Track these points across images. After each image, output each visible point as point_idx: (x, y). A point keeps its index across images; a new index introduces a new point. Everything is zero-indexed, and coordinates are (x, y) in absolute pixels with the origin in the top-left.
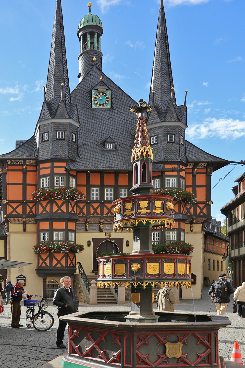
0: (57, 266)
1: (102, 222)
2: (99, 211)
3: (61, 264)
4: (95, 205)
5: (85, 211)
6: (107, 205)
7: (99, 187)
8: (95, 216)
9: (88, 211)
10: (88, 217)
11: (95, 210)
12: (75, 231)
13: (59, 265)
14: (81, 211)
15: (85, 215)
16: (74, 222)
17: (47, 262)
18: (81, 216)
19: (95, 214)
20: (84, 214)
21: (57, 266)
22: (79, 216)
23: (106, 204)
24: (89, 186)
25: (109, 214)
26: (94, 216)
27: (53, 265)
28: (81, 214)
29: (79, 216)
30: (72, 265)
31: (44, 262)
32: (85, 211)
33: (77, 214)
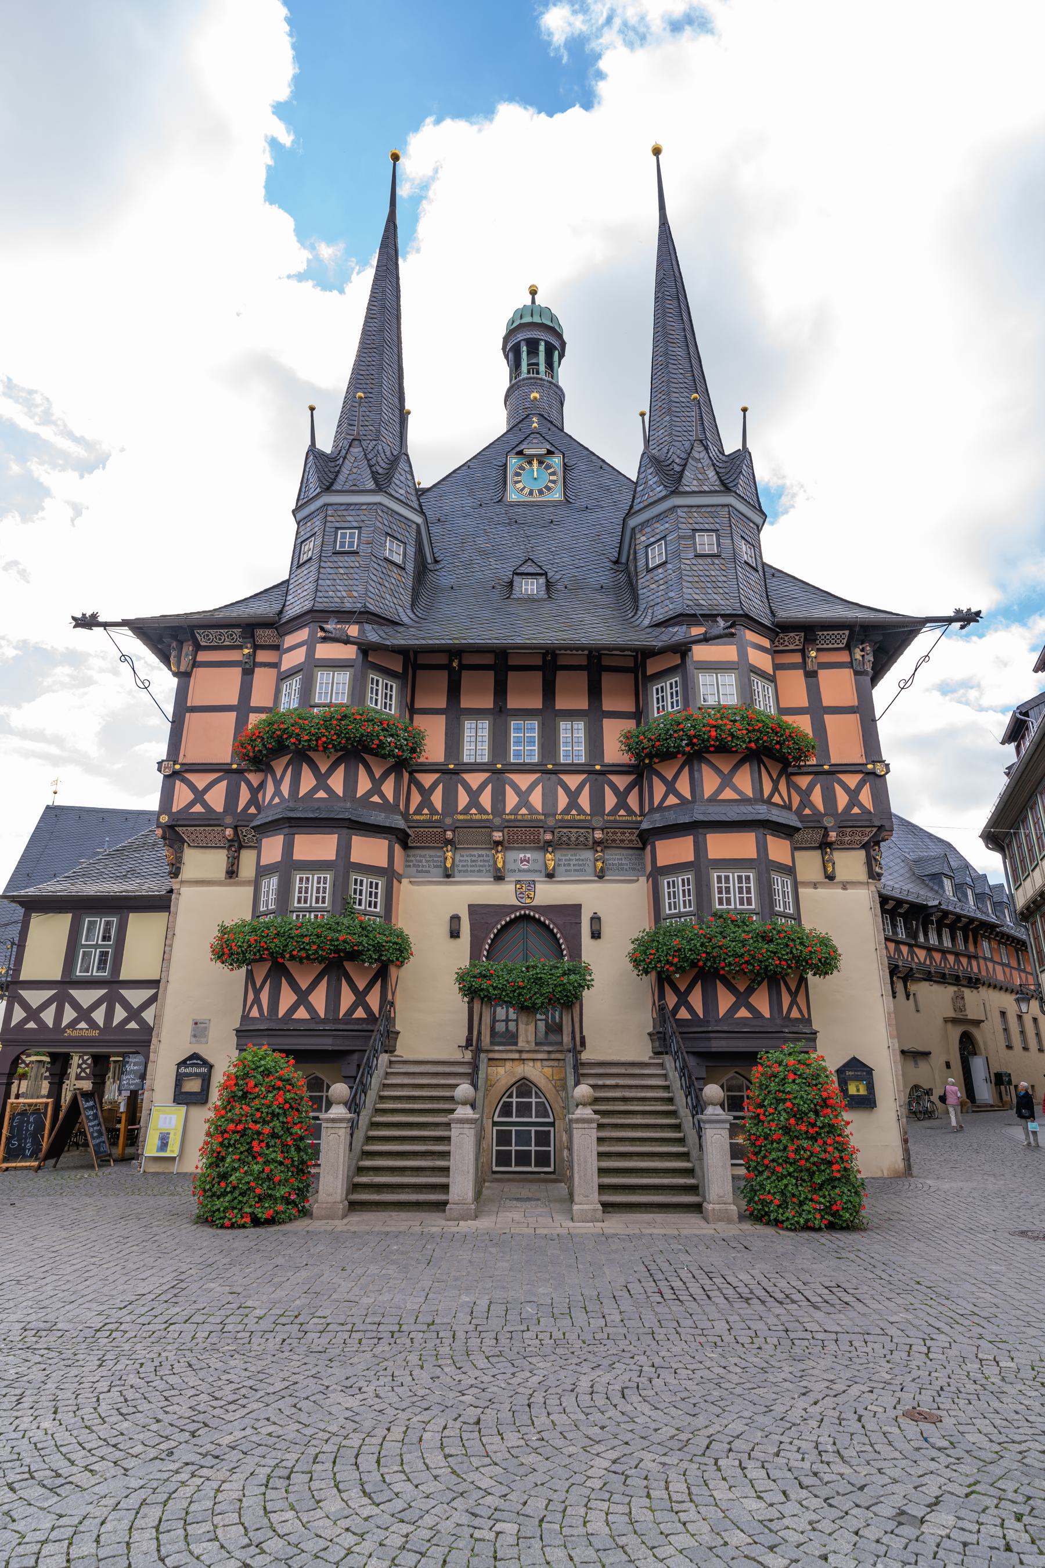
0: (297, 1016)
1: (498, 843)
2: (486, 799)
3: (310, 1008)
4: (474, 780)
5: (437, 799)
6: (515, 777)
7: (491, 717)
8: (474, 817)
9: (450, 798)
10: (448, 821)
11: (474, 795)
12: (389, 874)
13: (302, 1013)
14: (426, 802)
15: (438, 813)
16: (385, 838)
17: (264, 997)
18: (422, 818)
19: (474, 811)
20: (433, 811)
21: (295, 1016)
22: (418, 817)
23: (512, 776)
24: (455, 715)
25: (524, 811)
26: (468, 817)
27: (281, 1013)
28: (426, 811)
29: (418, 817)
30: (360, 1013)
31: (257, 992)
32: (437, 799)
33: (411, 812)
